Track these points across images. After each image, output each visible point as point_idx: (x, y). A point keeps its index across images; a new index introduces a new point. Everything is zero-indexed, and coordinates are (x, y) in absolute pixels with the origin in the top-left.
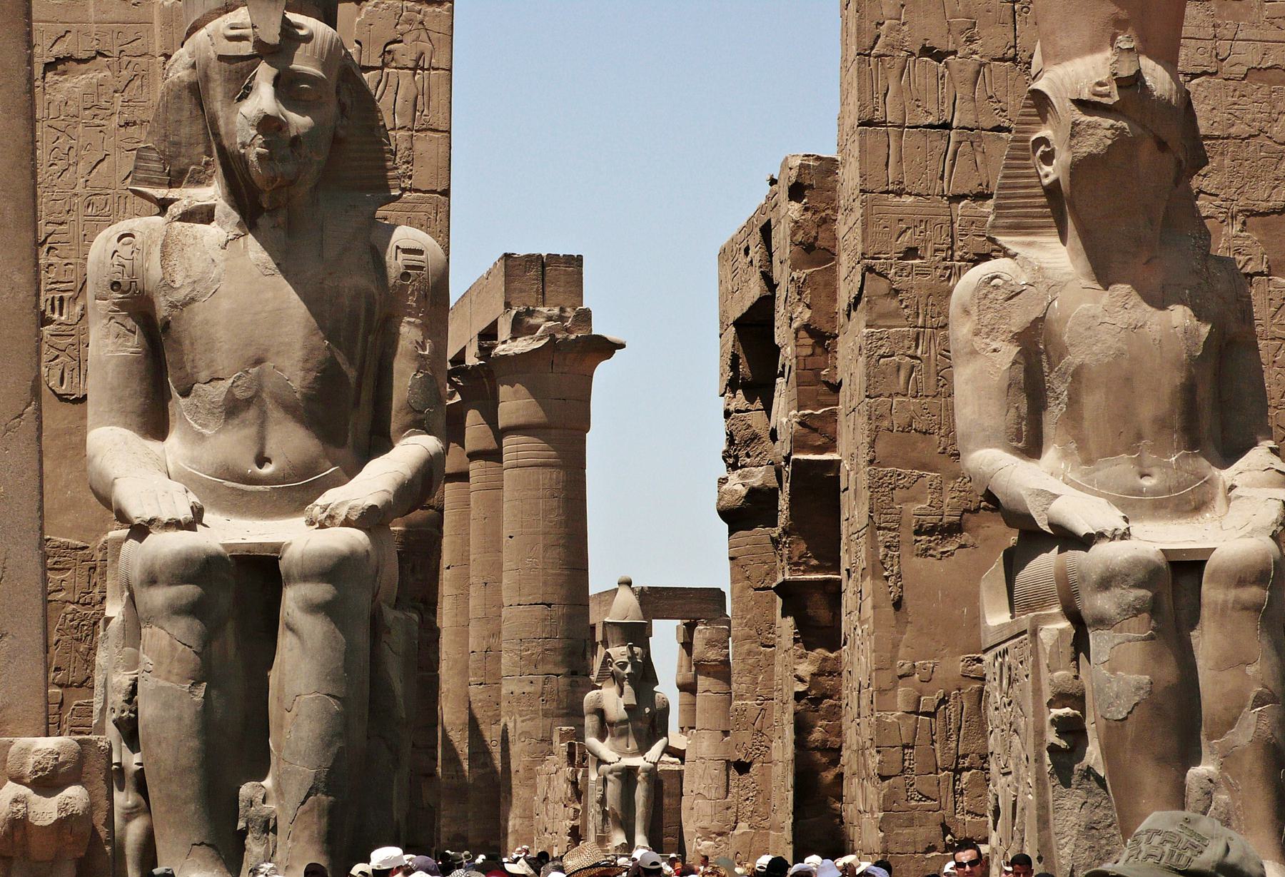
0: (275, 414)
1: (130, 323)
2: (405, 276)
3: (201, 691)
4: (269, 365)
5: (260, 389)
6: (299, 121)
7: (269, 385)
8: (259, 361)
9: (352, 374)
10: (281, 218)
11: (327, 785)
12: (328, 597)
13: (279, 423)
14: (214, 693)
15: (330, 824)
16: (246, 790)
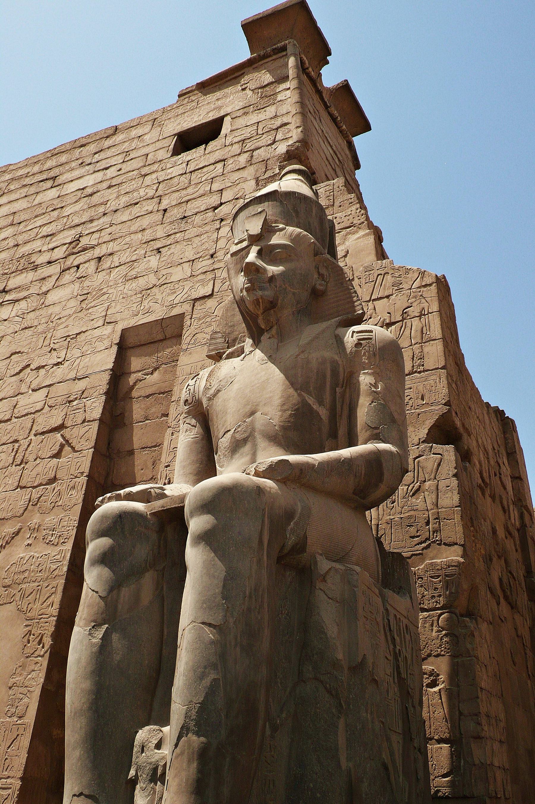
0: (262, 443)
1: (193, 421)
2: (358, 345)
3: (100, 633)
4: (258, 414)
5: (253, 430)
6: (273, 269)
7: (258, 426)
8: (252, 413)
9: (323, 413)
10: (274, 331)
11: (198, 724)
12: (208, 526)
13: (264, 449)
14: (115, 637)
15: (201, 771)
16: (142, 735)
